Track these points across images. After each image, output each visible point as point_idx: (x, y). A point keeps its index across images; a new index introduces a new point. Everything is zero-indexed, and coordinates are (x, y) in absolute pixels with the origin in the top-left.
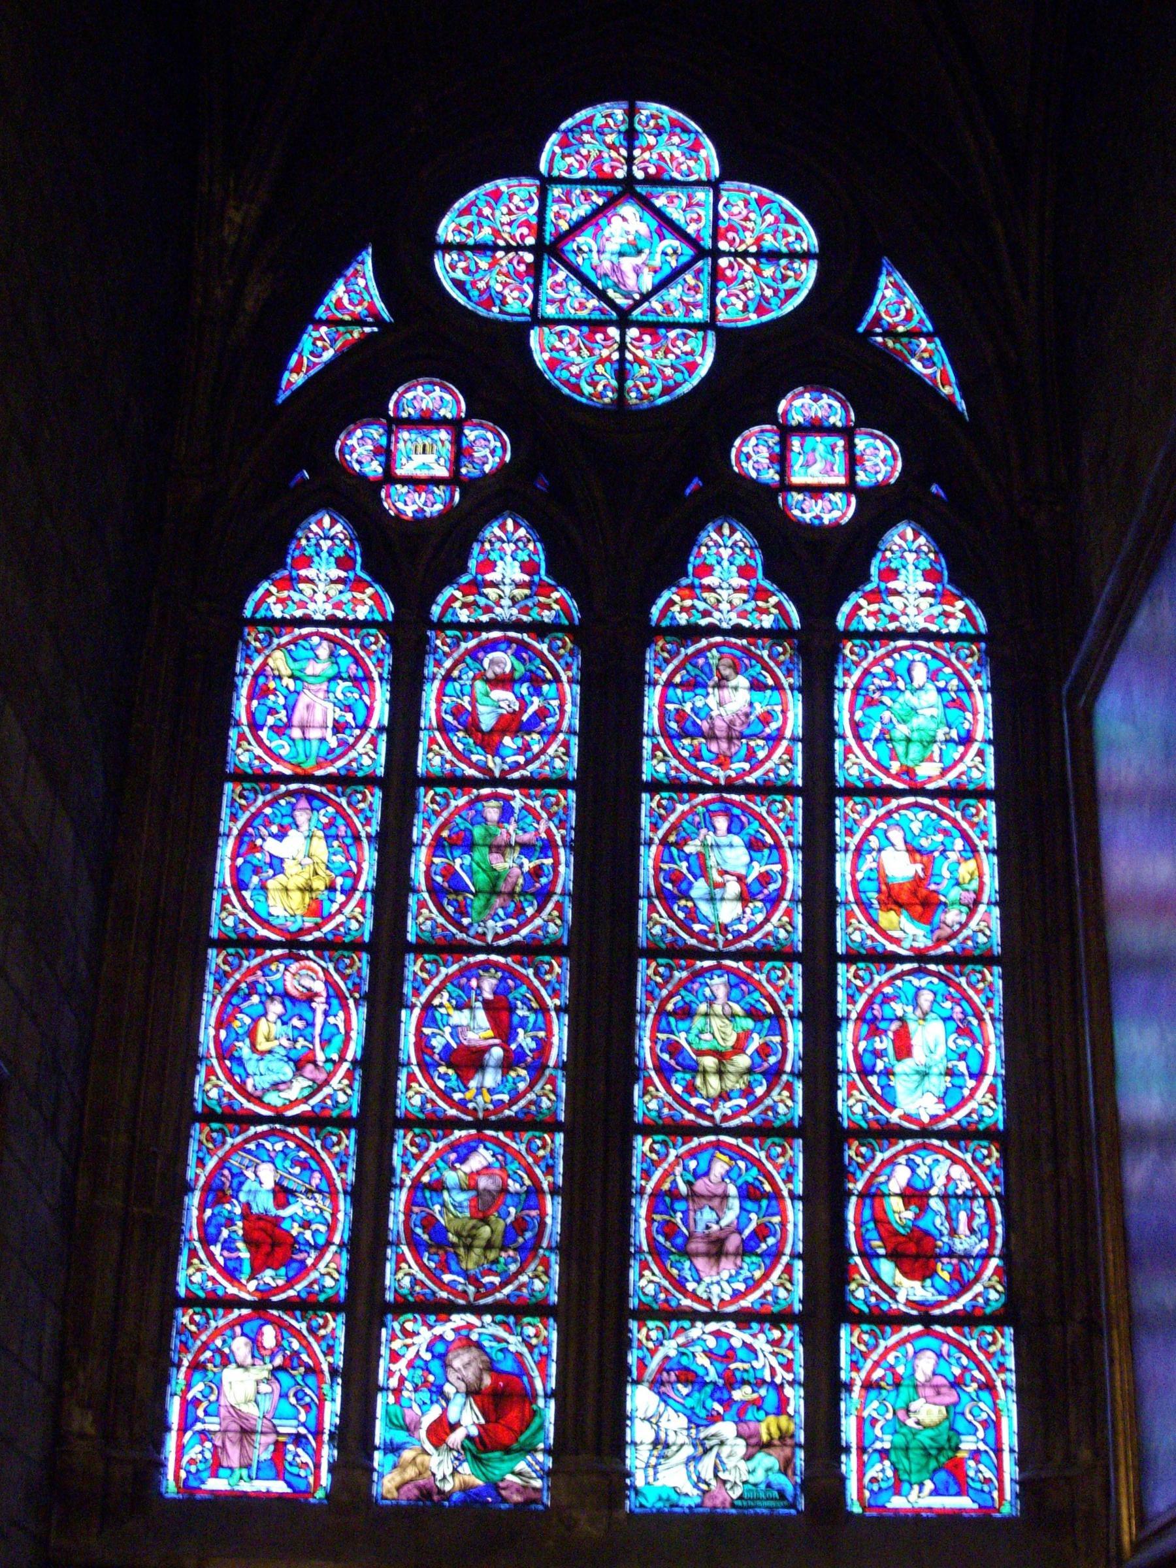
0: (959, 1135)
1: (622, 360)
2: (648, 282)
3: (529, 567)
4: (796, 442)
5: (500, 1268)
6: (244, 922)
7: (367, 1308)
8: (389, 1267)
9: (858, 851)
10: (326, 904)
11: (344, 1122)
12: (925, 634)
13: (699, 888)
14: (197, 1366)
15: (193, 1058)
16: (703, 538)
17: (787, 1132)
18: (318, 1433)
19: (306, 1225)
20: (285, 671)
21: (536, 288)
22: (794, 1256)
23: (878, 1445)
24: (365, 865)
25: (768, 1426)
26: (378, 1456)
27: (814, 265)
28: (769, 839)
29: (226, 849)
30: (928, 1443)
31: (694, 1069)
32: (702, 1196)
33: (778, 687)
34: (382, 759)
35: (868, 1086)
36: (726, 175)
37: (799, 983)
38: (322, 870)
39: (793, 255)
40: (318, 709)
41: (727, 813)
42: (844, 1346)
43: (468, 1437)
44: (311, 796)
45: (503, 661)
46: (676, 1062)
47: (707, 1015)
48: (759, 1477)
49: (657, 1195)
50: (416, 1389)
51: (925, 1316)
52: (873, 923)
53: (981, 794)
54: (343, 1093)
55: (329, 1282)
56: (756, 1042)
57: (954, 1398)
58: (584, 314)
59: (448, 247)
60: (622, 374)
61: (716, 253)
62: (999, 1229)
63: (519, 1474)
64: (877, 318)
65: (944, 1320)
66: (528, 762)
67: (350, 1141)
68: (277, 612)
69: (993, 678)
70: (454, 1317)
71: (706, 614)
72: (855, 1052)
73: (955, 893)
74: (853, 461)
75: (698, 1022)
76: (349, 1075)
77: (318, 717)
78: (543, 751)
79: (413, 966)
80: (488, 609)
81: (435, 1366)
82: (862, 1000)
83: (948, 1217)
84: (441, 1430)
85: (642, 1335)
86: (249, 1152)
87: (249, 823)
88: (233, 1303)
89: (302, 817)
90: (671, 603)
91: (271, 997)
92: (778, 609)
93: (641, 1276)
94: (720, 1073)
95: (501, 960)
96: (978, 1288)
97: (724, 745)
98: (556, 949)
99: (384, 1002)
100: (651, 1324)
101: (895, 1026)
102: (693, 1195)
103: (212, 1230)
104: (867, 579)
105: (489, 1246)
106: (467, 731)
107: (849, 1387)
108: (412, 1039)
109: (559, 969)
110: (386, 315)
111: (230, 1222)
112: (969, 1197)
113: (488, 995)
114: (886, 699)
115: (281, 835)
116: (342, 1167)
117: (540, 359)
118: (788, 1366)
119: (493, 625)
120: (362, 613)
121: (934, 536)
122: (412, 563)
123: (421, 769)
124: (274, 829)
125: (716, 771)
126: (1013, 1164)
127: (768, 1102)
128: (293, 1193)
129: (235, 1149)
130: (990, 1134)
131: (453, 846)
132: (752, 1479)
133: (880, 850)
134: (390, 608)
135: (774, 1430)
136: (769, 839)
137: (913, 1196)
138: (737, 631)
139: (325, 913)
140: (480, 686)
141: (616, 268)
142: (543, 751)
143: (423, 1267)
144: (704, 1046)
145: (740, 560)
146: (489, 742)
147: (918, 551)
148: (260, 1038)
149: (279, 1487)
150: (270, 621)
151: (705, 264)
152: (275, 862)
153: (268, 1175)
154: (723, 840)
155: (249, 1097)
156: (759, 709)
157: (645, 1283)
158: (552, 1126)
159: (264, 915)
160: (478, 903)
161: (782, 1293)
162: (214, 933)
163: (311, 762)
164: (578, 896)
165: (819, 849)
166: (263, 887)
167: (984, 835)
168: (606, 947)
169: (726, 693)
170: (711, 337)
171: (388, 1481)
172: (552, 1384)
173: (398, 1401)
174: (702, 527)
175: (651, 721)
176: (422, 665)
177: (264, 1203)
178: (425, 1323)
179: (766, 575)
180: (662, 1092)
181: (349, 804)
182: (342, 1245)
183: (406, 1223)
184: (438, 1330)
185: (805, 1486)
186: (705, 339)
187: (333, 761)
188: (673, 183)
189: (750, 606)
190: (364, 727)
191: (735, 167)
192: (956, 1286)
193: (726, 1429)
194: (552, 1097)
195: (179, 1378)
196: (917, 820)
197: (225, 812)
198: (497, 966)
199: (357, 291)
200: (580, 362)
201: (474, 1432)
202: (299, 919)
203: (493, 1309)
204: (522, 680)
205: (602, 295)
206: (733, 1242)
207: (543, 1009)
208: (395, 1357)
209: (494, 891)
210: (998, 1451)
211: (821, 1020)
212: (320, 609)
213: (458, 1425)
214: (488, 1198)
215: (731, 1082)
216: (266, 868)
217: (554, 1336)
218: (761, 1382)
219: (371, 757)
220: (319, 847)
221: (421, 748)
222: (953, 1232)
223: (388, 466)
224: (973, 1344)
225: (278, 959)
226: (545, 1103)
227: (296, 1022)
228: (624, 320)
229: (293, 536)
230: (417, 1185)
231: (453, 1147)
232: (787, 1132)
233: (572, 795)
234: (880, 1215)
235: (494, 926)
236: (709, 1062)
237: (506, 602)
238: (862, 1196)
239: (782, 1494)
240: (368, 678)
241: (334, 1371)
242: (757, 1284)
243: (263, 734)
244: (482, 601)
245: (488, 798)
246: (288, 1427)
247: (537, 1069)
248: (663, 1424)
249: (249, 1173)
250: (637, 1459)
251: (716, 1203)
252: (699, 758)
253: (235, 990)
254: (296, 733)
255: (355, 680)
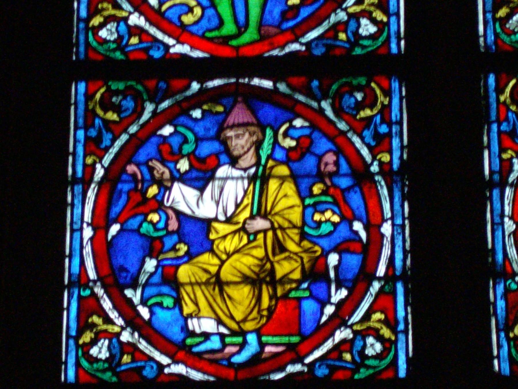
6: (131, 348)
10: (309, 306)
89: (240, 141)
124: (184, 165)
139: (309, 326)
152: (188, 228)
159: (175, 333)
163: (250, 35)
181: (338, 111)
187: (296, 34)
202: (252, 338)
216: (169, 243)
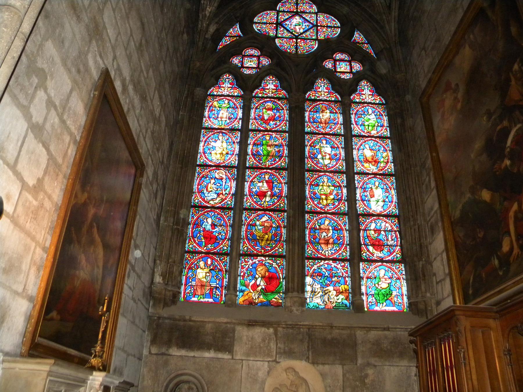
0: (387, 216)
1: (297, 45)
2: (302, 31)
3: (276, 86)
4: (338, 63)
5: (271, 245)
7: (235, 255)
8: (241, 245)
9: (358, 149)
11: (230, 209)
12: (370, 103)
13: (319, 156)
14: (190, 268)
15: (192, 192)
16: (317, 81)
17: (344, 214)
18: (222, 287)
19: (220, 234)
20: (217, 106)
21: (276, 31)
22: (347, 245)
23: (371, 293)
24: (236, 149)
25: (342, 287)
26: (238, 293)
27: (339, 29)
28: (336, 146)
29: (201, 144)
30: (384, 293)
31: (320, 199)
32: (323, 229)
33: (336, 113)
34: (240, 125)
35: (364, 204)
36: (319, 12)
37: (345, 179)
38: (225, 149)
39: (334, 27)
40: (224, 114)
41: (326, 140)
42: (361, 267)
43: (262, 288)
44: (222, 133)
45: (270, 105)
46: (314, 196)
47: (322, 185)
48: (340, 301)
49: (311, 229)
50: (248, 276)
51: (382, 260)
52: (363, 166)
53: (387, 138)
54: (230, 202)
55: (225, 248)
56: (335, 192)
57: (390, 281)
58: (287, 36)
59: (256, 23)
60: (297, 48)
61: (317, 26)
62: (399, 239)
63: (275, 299)
64: (355, 40)
65: (387, 262)
66: (276, 127)
67: (231, 213)
68: (215, 93)
69: (387, 113)
70: (259, 258)
71: (318, 97)
72: (360, 195)
73: (382, 160)
74: (351, 68)
75: (321, 187)
76: (232, 197)
77: (225, 116)
78: (280, 125)
79: (248, 172)
80: (266, 94)
81: (253, 270)
82: (361, 183)
83: (386, 236)
84: (255, 287)
85: (308, 264)
86: (205, 215)
87: (207, 138)
88: (200, 253)
89: (220, 138)
90: (310, 94)
91: (212, 178)
92: (335, 96)
93: (307, 249)
94: (326, 199)
95: (270, 171)
96: (395, 254)
97: (324, 125)
98: (284, 169)
99: (240, 180)
100: (310, 261)
101: (370, 189)
102: (320, 229)
103: (195, 234)
104: (357, 91)
105: (267, 240)
106: (262, 120)
107: (363, 278)
108: (247, 189)
109: (285, 173)
110: (242, 35)
111: (200, 233)
112: (391, 231)
113: (267, 179)
114: (363, 116)
115: (216, 141)
116: (229, 220)
117: (278, 45)
118: (347, 273)
119: (267, 97)
120: (236, 94)
121: (370, 82)
122: (248, 85)
123: (250, 127)
125: (322, 130)
126: (402, 223)
127: (339, 207)
128: (216, 225)
129: (202, 214)
130: (395, 216)
131: (258, 145)
132: (338, 301)
133: (363, 149)
134: (242, 93)
135: (343, 288)
136: (336, 146)
137: (376, 230)
138: (326, 101)
140: (264, 110)
141: (295, 28)
142: (280, 125)
143: (250, 245)
144: (322, 193)
145: (326, 86)
146: (267, 122)
147: (368, 86)
148: (209, 188)
149: (211, 300)
150: (214, 95)
151: (315, 28)
153: (210, 221)
154: (325, 146)
155: (206, 202)
156: (332, 117)
157: (309, 251)
158: (284, 211)
160: (264, 158)
161: (344, 254)
162: (198, 163)
164: (289, 156)
165: (348, 149)
166: (211, 153)
167: (388, 147)
168: (297, 167)
169: (324, 114)
170: (317, 42)
171: (241, 300)
172: (284, 275)
173: (243, 279)
174: (317, 79)
175: (307, 119)
176: (250, 105)
177: (209, 227)
178: (250, 259)
179: (332, 89)
180: (312, 203)
182: (229, 239)
183: (246, 234)
184: (254, 261)
185: (352, 303)
186: (315, 42)
188: (307, 13)
189: (329, 96)
190: (236, 118)
191: (320, 10)
192: (389, 253)
193: (331, 288)
194: (284, 204)
195: (185, 272)
196: (371, 143)
197: (202, 136)
198: (269, 172)
199: (236, 30)
200: (286, 45)
201: (263, 287)
203: (269, 256)
204: (274, 109)
205: (292, 33)
206: (331, 241)
207: (281, 183)
208: (243, 267)
209: (268, 155)
210: (402, 295)
211: (351, 187)
212: (226, 93)
213: (260, 285)
214: (267, 228)
215: (329, 202)
217: (285, 263)
218: (340, 276)
219: (238, 125)
220: (225, 145)
221: (250, 123)
222: (387, 240)
223: (242, 65)
224: (394, 268)
225: (214, 170)
226: (282, 205)
227: (218, 184)
228: (297, 38)
229: (219, 78)
230: (248, 224)
231: (258, 215)
232: (344, 214)
233: (287, 134)
234: (369, 235)
235: (268, 164)
236: (324, 197)
237: (270, 93)
238: (363, 230)
239: (346, 305)
240: (237, 108)
241: (226, 271)
242: (338, 251)
243: (211, 119)
244: (265, 92)
245: (266, 135)
246: (214, 285)
247: (280, 197)
248: (314, 286)
249: (205, 220)
250: (308, 295)
251: (326, 231)
252: (318, 127)
253: (203, 177)
254: (219, 119)
255: (233, 108)
